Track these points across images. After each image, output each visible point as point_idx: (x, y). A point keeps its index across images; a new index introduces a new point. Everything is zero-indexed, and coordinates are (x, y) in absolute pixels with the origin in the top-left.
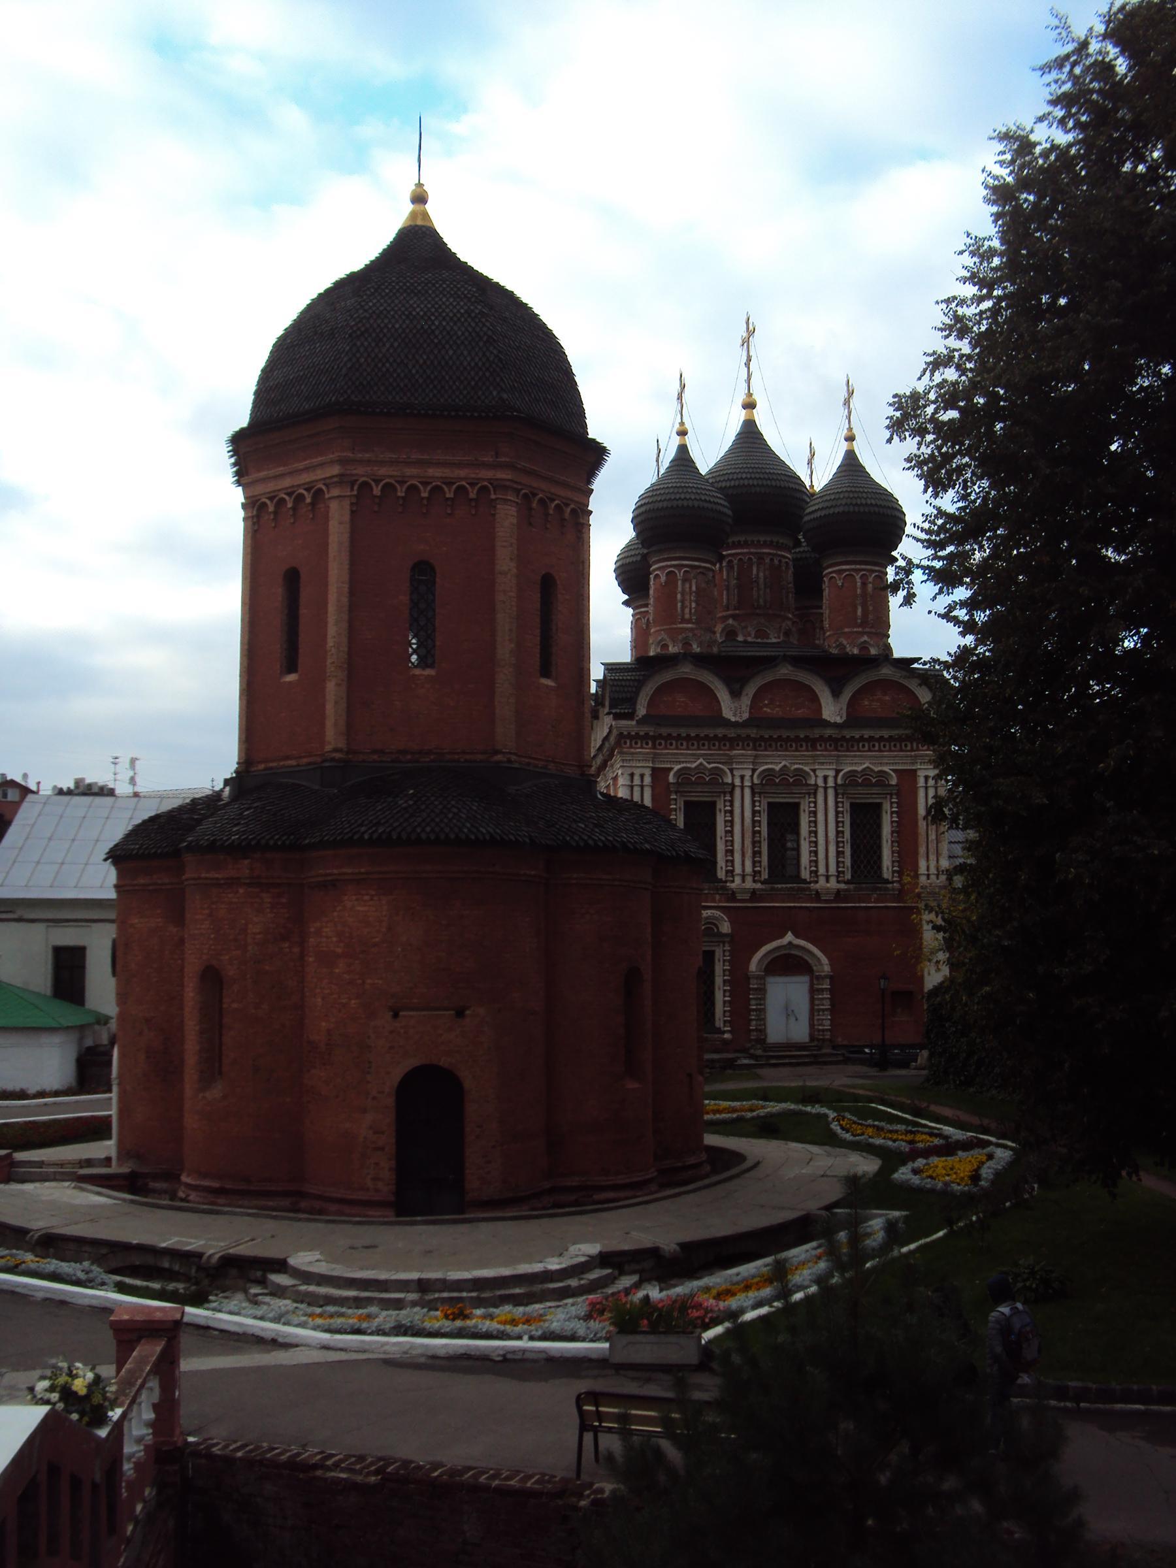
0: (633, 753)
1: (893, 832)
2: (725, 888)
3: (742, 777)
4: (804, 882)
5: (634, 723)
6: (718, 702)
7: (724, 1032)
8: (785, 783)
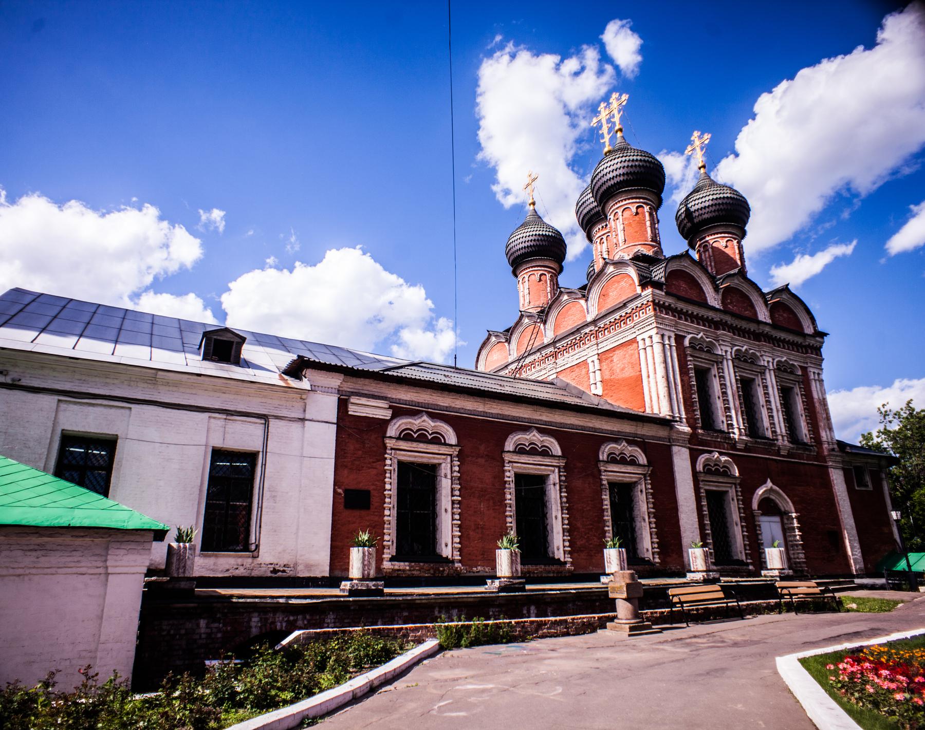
0: (663, 318)
4: (768, 439)
7: (748, 564)
8: (745, 361)
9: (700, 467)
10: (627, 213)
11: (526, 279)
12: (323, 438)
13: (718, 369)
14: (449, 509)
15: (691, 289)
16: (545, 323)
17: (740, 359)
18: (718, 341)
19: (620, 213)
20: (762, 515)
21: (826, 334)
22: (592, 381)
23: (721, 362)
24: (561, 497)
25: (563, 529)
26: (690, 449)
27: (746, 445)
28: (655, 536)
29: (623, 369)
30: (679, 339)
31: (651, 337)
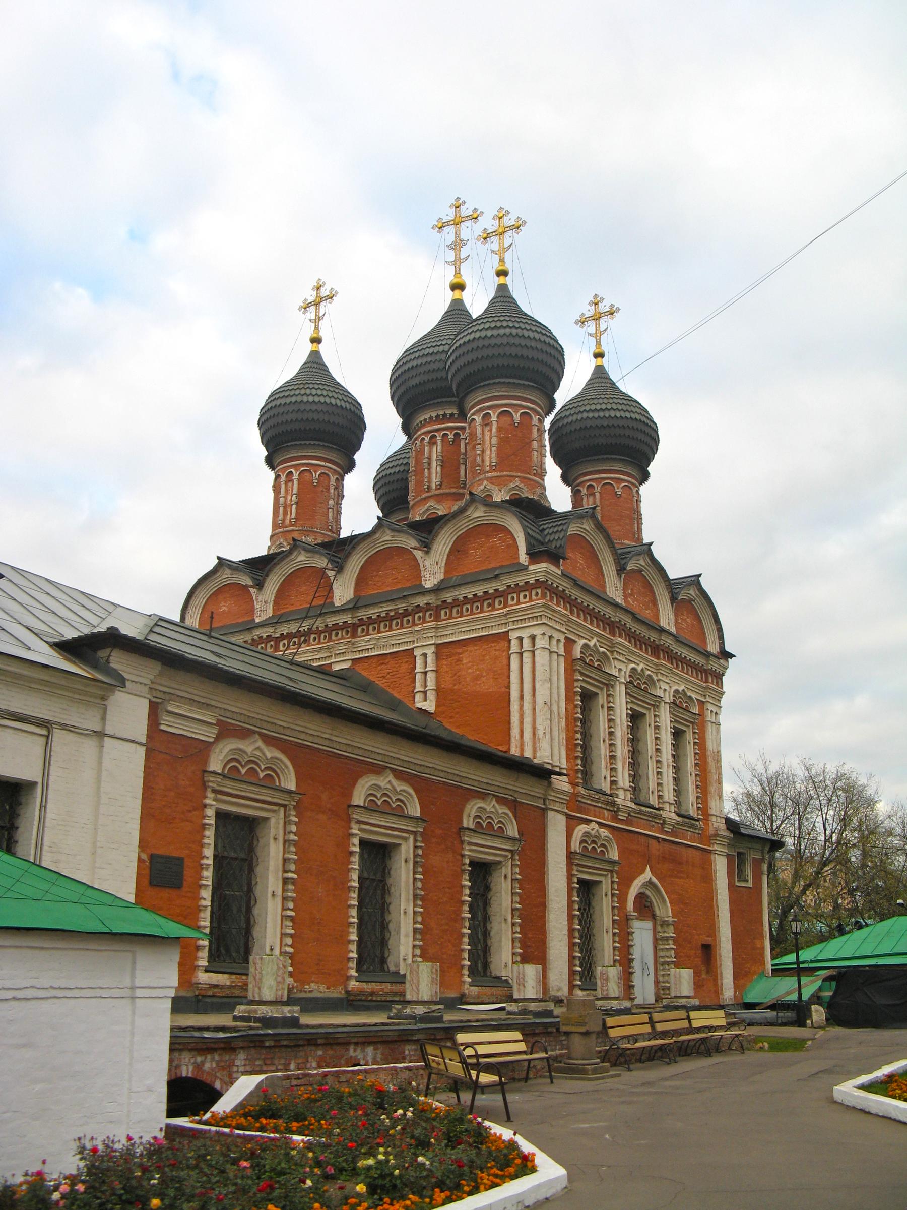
0: (554, 611)
1: (696, 765)
2: (614, 804)
3: (620, 670)
4: (652, 807)
5: (560, 573)
6: (603, 575)
9: (576, 846)
10: (505, 420)
11: (296, 476)
12: (127, 766)
13: (608, 695)
14: (279, 892)
15: (588, 567)
16: (340, 569)
17: (639, 686)
18: (612, 652)
19: (494, 418)
20: (637, 919)
21: (731, 656)
22: (418, 687)
23: (613, 686)
24: (415, 879)
25: (415, 930)
26: (568, 817)
27: (629, 815)
28: (518, 945)
29: (476, 678)
30: (569, 643)
31: (533, 638)
